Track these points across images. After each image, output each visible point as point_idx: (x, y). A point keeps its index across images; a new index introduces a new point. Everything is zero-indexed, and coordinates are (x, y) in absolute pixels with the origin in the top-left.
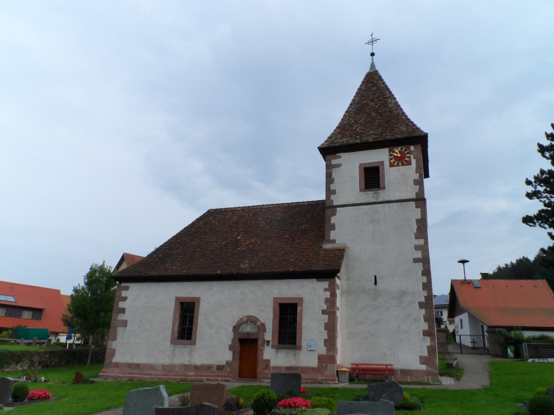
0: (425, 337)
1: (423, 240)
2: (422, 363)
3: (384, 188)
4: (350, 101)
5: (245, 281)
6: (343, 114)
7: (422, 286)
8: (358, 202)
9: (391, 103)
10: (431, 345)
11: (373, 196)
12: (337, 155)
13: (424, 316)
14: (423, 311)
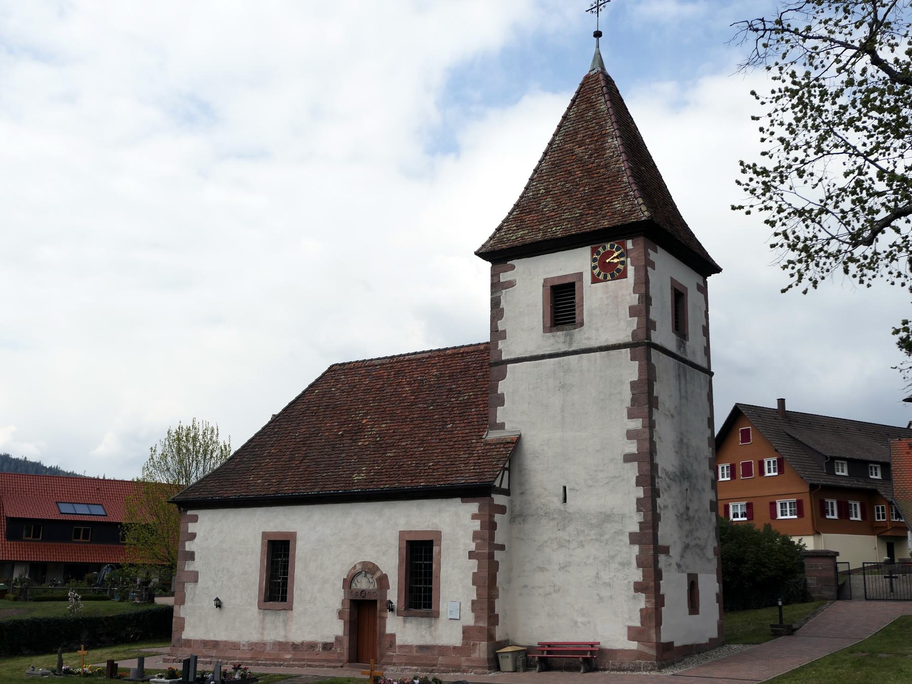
0: (636, 594)
1: (641, 419)
2: (631, 638)
3: (582, 324)
4: (544, 147)
5: (359, 503)
6: (529, 177)
7: (637, 504)
8: (541, 352)
9: (610, 148)
10: (646, 607)
11: (563, 341)
12: (509, 264)
13: (638, 558)
14: (636, 549)
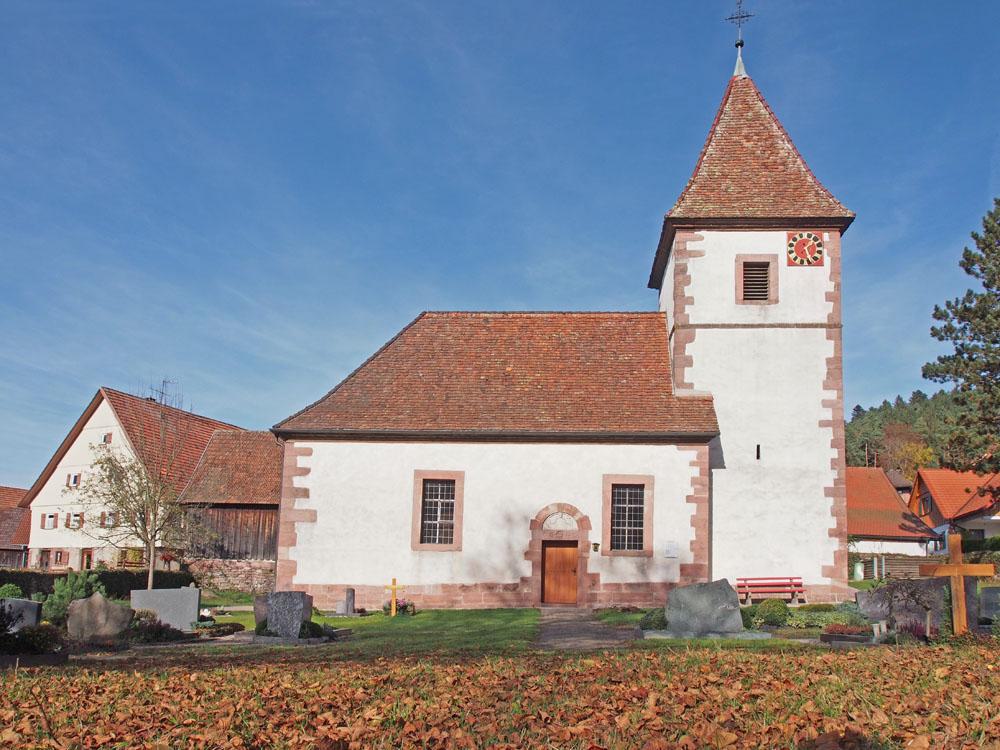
3: (777, 301)
8: (734, 322)
13: (832, 509)
14: (830, 501)
